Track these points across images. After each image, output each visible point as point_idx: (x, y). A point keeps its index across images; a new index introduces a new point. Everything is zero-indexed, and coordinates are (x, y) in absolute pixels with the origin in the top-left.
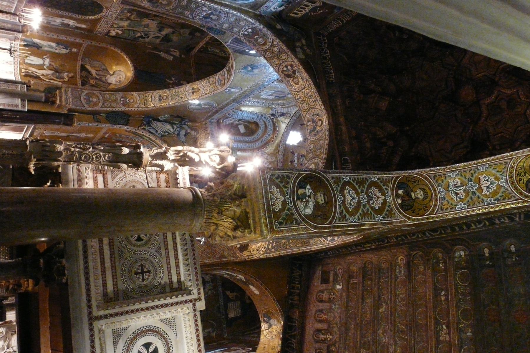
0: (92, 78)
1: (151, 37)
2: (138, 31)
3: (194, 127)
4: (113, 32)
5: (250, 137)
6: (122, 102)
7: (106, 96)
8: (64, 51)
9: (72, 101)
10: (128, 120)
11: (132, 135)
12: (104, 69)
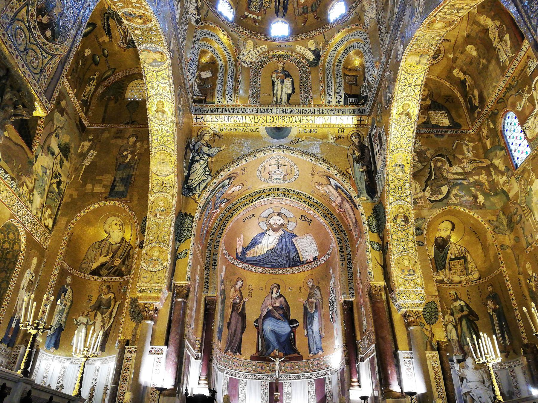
0: (113, 262)
1: (60, 171)
2: (51, 184)
3: (199, 135)
4: (47, 220)
5: (220, 66)
6: (163, 217)
7: (152, 238)
8: (69, 294)
9: (157, 283)
10: (186, 214)
11: (204, 213)
12: (100, 246)
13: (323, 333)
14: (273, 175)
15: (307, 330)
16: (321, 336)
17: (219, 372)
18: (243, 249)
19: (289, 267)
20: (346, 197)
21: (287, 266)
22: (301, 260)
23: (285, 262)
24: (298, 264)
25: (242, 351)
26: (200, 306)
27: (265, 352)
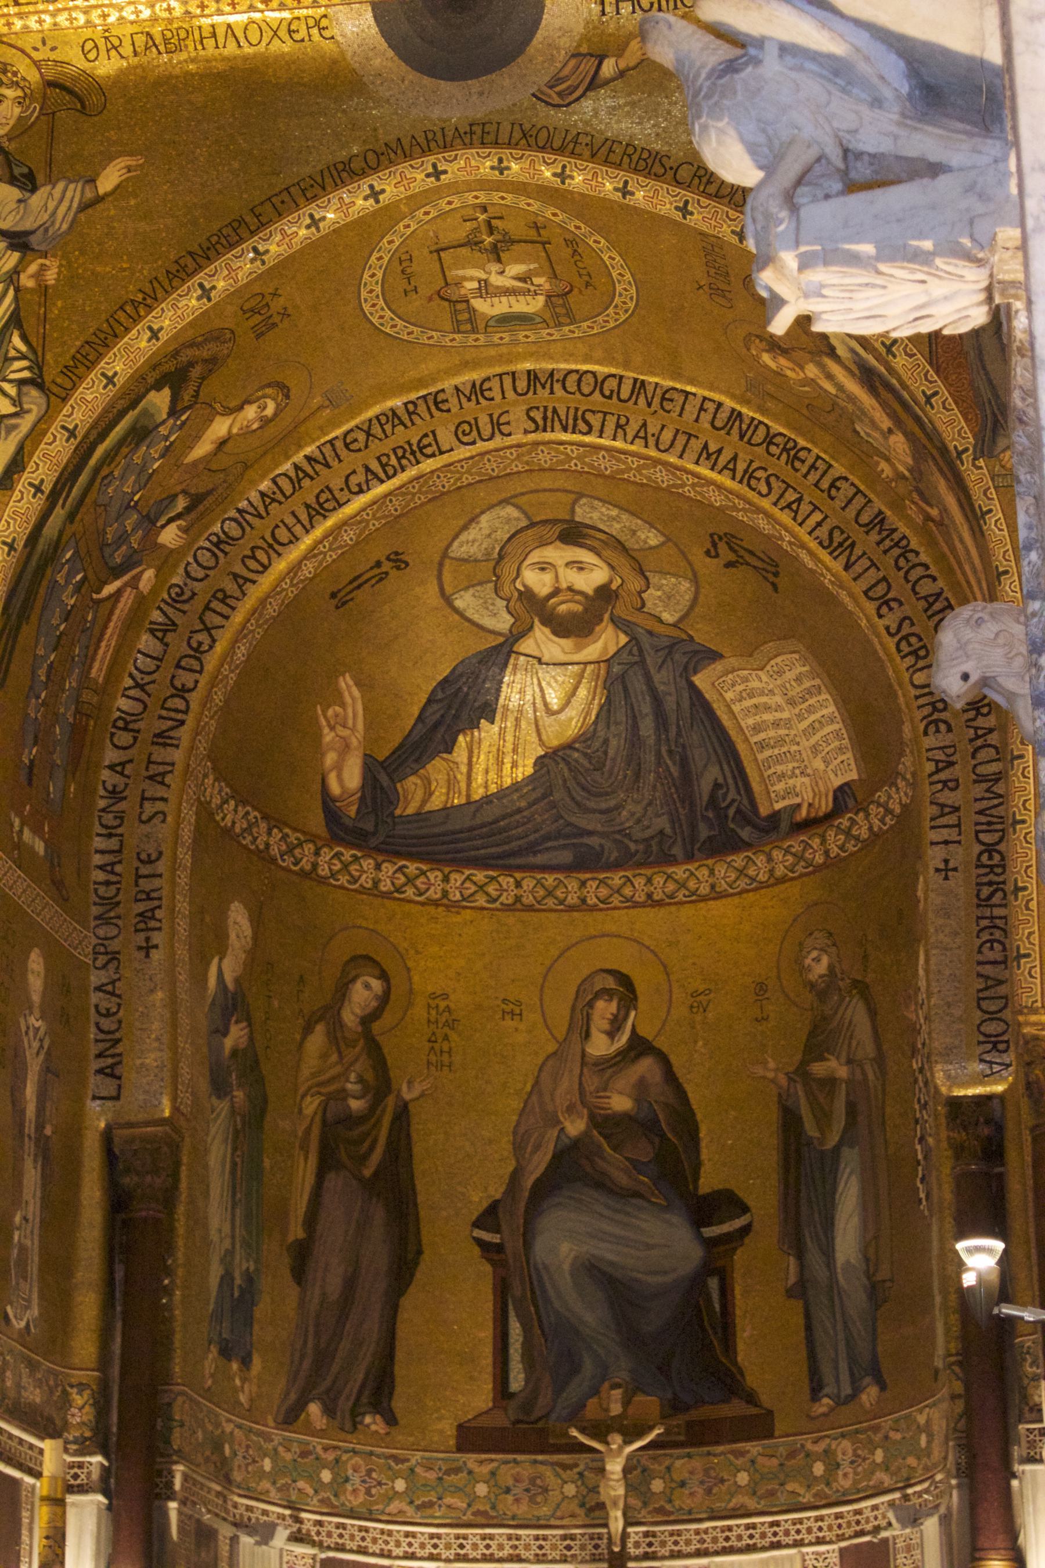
13: (883, 1273)
14: (478, 304)
15: (800, 1256)
16: (876, 1293)
17: (246, 1540)
18: (370, 766)
19: (690, 858)
20: (929, 446)
21: (677, 851)
22: (764, 811)
23: (662, 823)
24: (745, 833)
25: (398, 1404)
26: (73, 1183)
27: (544, 1401)
